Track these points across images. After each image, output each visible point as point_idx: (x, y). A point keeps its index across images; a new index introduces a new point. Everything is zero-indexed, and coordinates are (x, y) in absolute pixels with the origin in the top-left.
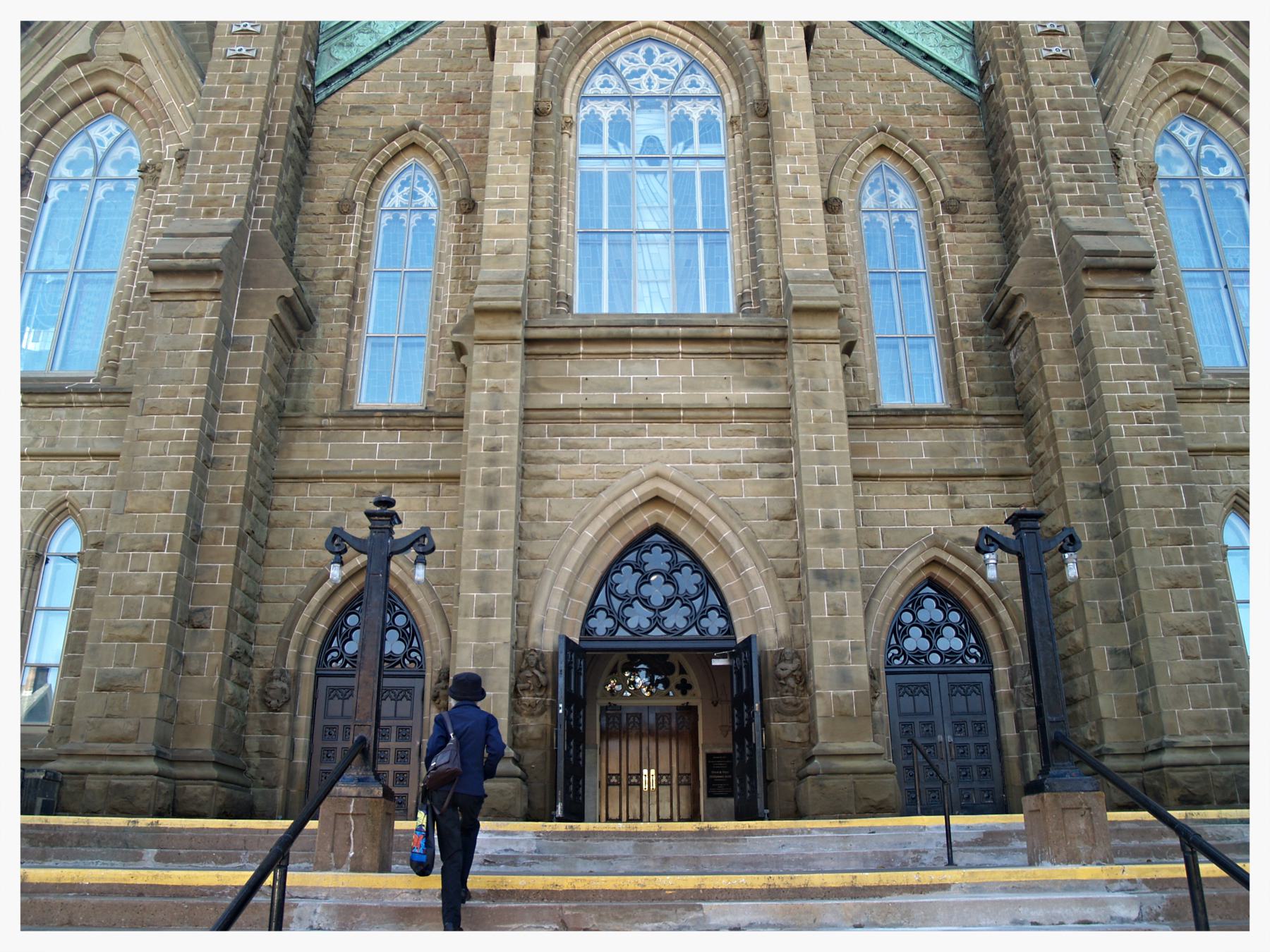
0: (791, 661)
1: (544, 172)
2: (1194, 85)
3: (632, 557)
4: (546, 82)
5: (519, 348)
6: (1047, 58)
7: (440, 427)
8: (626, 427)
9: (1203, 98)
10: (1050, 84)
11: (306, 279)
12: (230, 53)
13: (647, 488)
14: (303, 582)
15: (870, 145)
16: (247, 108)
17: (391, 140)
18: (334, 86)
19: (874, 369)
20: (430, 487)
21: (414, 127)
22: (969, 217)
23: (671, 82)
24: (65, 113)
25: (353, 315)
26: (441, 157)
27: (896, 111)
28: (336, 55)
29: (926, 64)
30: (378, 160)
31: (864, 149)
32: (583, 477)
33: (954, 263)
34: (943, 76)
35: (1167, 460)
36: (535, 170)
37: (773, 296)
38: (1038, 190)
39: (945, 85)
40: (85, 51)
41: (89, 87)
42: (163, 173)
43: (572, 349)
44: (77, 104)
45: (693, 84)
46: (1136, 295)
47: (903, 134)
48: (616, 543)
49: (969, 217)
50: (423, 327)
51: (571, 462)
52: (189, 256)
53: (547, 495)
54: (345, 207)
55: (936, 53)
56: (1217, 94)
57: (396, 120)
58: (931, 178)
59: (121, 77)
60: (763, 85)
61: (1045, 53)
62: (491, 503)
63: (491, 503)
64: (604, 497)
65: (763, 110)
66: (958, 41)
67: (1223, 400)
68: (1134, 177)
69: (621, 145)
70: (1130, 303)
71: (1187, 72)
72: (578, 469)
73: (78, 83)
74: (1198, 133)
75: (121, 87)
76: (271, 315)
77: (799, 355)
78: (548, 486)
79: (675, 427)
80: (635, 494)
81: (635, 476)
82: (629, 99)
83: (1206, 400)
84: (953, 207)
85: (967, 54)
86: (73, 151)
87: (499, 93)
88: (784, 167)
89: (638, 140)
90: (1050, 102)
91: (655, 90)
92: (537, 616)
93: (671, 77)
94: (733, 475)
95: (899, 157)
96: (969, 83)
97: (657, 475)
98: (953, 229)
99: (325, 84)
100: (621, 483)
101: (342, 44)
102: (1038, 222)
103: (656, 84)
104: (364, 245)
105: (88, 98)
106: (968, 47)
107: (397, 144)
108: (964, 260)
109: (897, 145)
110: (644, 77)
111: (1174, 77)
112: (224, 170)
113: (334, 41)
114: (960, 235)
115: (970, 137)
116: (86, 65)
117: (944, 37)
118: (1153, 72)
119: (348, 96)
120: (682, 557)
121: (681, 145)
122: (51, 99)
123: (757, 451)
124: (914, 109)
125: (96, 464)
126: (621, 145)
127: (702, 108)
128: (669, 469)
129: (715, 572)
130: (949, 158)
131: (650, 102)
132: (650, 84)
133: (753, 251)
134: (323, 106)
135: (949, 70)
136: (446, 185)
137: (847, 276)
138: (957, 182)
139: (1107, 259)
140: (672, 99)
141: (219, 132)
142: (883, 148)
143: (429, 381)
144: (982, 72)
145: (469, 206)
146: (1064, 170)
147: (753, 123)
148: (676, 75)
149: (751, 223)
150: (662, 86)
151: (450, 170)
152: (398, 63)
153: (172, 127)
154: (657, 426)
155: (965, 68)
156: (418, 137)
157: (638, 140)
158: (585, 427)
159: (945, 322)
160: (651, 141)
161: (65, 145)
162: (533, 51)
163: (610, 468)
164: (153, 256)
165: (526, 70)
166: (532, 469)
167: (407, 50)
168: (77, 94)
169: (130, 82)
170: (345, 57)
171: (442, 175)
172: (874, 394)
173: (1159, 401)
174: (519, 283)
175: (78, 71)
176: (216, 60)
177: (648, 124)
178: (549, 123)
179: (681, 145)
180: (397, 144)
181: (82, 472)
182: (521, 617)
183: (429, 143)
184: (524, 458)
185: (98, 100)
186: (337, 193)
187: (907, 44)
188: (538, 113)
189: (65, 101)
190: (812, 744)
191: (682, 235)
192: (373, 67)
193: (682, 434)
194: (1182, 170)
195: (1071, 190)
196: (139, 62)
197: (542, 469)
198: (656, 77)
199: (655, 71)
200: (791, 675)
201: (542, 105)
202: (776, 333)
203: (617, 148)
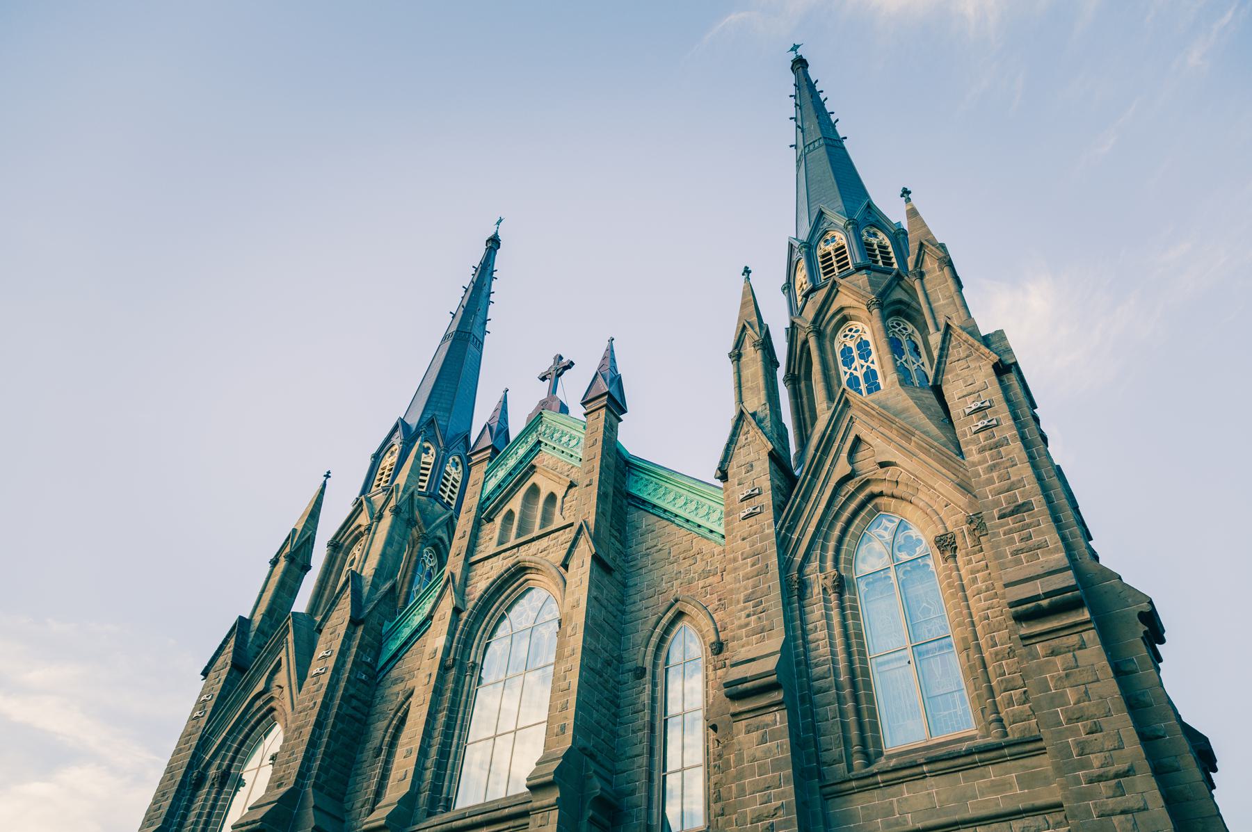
10: (743, 539)
18: (388, 668)
46: (771, 710)
67: (876, 786)
70: (768, 718)
83: (862, 789)
99: (383, 668)
113: (390, 638)
122: (245, 725)
134: (382, 684)
139: (739, 686)
170: (394, 646)
175: (259, 703)
192: (409, 648)
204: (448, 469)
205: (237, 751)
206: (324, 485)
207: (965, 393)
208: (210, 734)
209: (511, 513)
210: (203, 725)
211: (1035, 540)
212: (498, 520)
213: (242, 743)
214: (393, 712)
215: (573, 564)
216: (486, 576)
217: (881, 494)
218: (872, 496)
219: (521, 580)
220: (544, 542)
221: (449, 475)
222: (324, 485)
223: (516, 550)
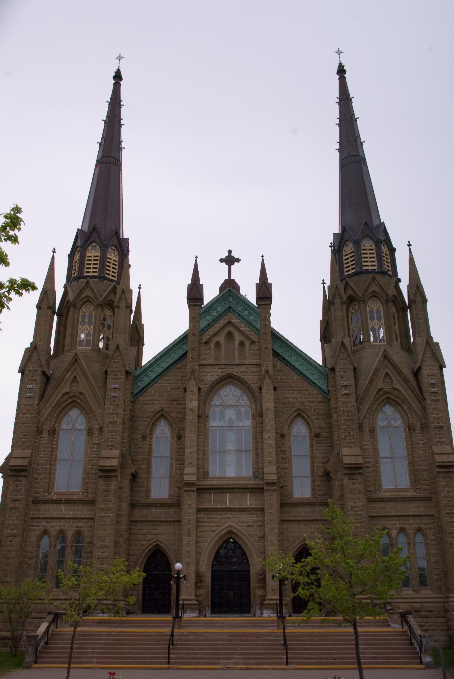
0: (262, 575)
1: (200, 436)
2: (390, 396)
3: (224, 545)
4: (201, 406)
5: (195, 493)
6: (343, 394)
7: (174, 506)
8: (223, 513)
9: (393, 400)
11: (135, 460)
12: (111, 396)
13: (228, 529)
14: (140, 550)
15: (295, 414)
16: (118, 414)
17: (156, 414)
18: (138, 395)
19: (292, 487)
20: (172, 524)
21: (163, 410)
22: (322, 438)
23: (237, 399)
24: (64, 408)
25: (148, 471)
26: (171, 420)
27: (304, 402)
28: (139, 385)
29: (313, 385)
30: (153, 421)
31: (292, 417)
32: (212, 526)
33: (316, 454)
34: (318, 389)
35: (360, 522)
36: (198, 435)
37: (262, 474)
38: (338, 437)
39: (318, 392)
40: (68, 391)
41: (70, 401)
42: (94, 431)
43: (209, 491)
44: (66, 406)
45: (243, 400)
47: (305, 410)
48: (221, 543)
49: (322, 438)
50: (168, 475)
51: (209, 522)
52: (109, 466)
53: (202, 531)
54: (144, 437)
55: (316, 382)
56: (397, 400)
57: (157, 407)
58: (312, 426)
59: (79, 398)
60: (261, 408)
61: (343, 393)
62: (189, 535)
63: (189, 535)
64: (217, 532)
65: (261, 415)
66: (323, 377)
68: (367, 430)
69: (222, 421)
71: (388, 392)
72: (211, 524)
73: (67, 400)
74: (392, 409)
75: (79, 401)
76: (129, 479)
77: (267, 495)
78: (203, 529)
79: (235, 513)
80: (225, 531)
81: (224, 526)
82: (224, 406)
84: (318, 436)
85: (326, 382)
86: (65, 419)
87: (187, 411)
88: (266, 435)
89: (227, 419)
90: (343, 410)
91: (232, 403)
92: (201, 563)
93: (236, 397)
94: (249, 526)
95: (303, 418)
96: (326, 393)
97: (230, 526)
98: (317, 443)
99: (136, 395)
100: (221, 528)
101: (140, 381)
102: (337, 448)
103: (232, 400)
104: (150, 448)
105: (69, 404)
106: (326, 380)
107: (158, 415)
108: (319, 453)
109: (303, 414)
110: (229, 398)
111: (384, 394)
112: (113, 435)
114: (319, 445)
115: (325, 411)
116: (69, 395)
117: (319, 376)
118: (377, 394)
119: (142, 398)
120: (237, 545)
121: (239, 421)
123: (255, 519)
124: (308, 402)
125: (86, 521)
126: (222, 421)
127: (245, 409)
128: (233, 524)
129: (245, 550)
130: (318, 419)
131: (230, 406)
132: (230, 400)
133: (257, 458)
134: (136, 402)
135: (320, 388)
136: (172, 428)
137: (286, 459)
138: (320, 428)
140: (237, 406)
141: (111, 423)
142: (299, 415)
143: (170, 491)
144: (329, 391)
145: (179, 437)
146: (345, 433)
147: (258, 418)
148: (238, 397)
149: (257, 449)
150: (234, 400)
151: (173, 424)
152: (156, 386)
153: (95, 416)
154: (230, 513)
155: (324, 387)
156: (164, 413)
157: (227, 419)
158: (212, 513)
159: (313, 472)
160: (231, 419)
161: (63, 417)
162: (197, 397)
163: (218, 524)
164: (100, 466)
165: (195, 403)
166: (200, 540)
167: (159, 382)
168: (66, 403)
169: (81, 400)
170: (142, 385)
171: (171, 425)
172: (292, 495)
173: (360, 506)
174: (195, 474)
175: (66, 397)
176: (107, 397)
177: (230, 414)
178: (202, 420)
179: (239, 421)
180: (158, 415)
181: (82, 523)
182: (197, 563)
183: (167, 415)
184: (197, 521)
185: (72, 404)
186: (141, 432)
187: (308, 378)
188: (199, 417)
189: (63, 406)
190: (266, 596)
191: (239, 452)
193: (237, 514)
194: (385, 424)
195: (345, 439)
196: (84, 395)
197: (201, 524)
198: (232, 398)
199: (232, 395)
200: (262, 579)
201: (200, 414)
202: (261, 486)
203: (221, 422)
204: (109, 256)
205: (57, 418)
206: (53, 258)
207: (429, 374)
208: (41, 408)
209: (218, 344)
210: (37, 403)
211: (443, 439)
212: (212, 345)
213: (58, 415)
214: (150, 418)
215: (265, 388)
216: (211, 374)
217: (391, 398)
218: (388, 398)
219: (227, 381)
220: (243, 369)
221: (110, 259)
222: (53, 258)
223: (226, 366)
